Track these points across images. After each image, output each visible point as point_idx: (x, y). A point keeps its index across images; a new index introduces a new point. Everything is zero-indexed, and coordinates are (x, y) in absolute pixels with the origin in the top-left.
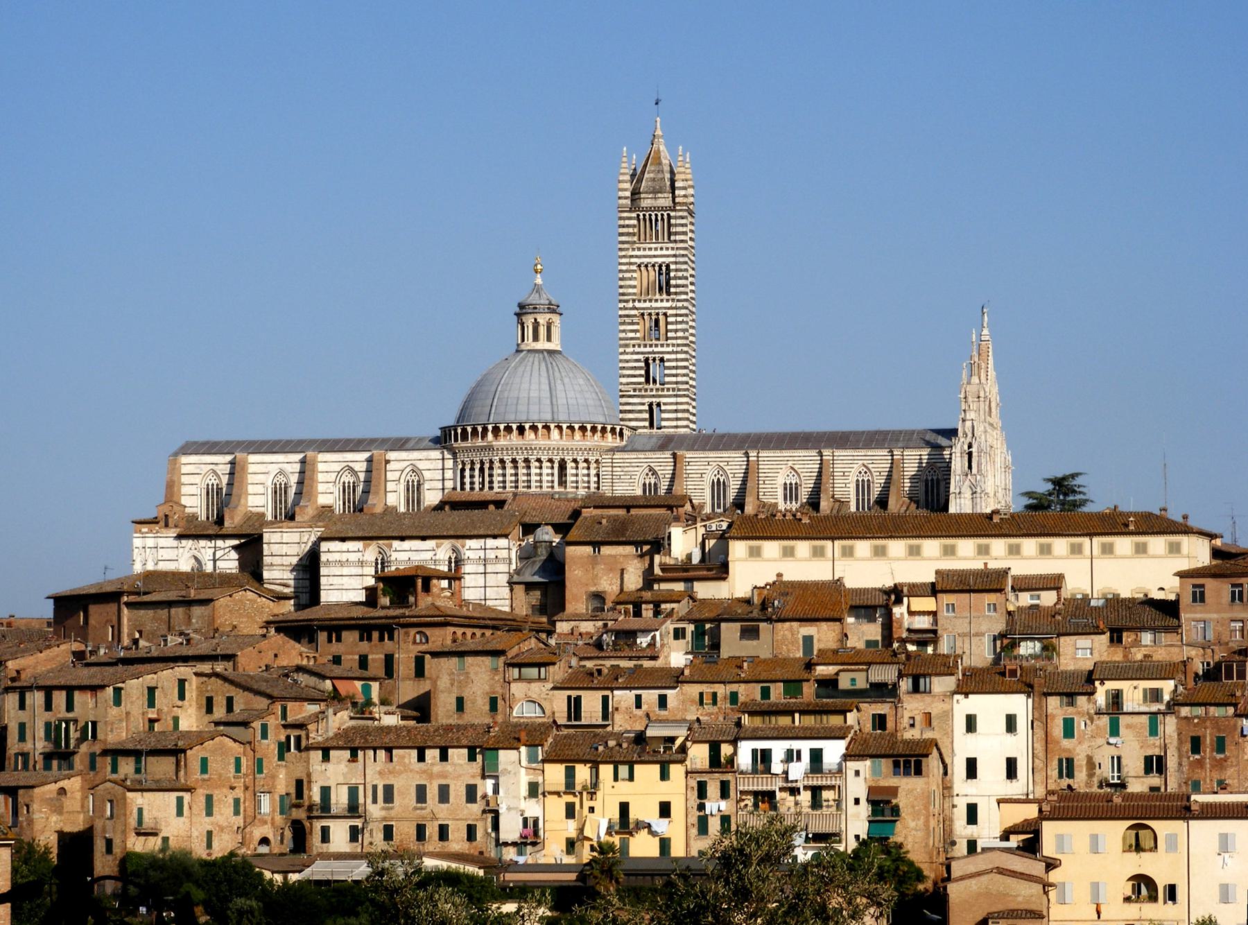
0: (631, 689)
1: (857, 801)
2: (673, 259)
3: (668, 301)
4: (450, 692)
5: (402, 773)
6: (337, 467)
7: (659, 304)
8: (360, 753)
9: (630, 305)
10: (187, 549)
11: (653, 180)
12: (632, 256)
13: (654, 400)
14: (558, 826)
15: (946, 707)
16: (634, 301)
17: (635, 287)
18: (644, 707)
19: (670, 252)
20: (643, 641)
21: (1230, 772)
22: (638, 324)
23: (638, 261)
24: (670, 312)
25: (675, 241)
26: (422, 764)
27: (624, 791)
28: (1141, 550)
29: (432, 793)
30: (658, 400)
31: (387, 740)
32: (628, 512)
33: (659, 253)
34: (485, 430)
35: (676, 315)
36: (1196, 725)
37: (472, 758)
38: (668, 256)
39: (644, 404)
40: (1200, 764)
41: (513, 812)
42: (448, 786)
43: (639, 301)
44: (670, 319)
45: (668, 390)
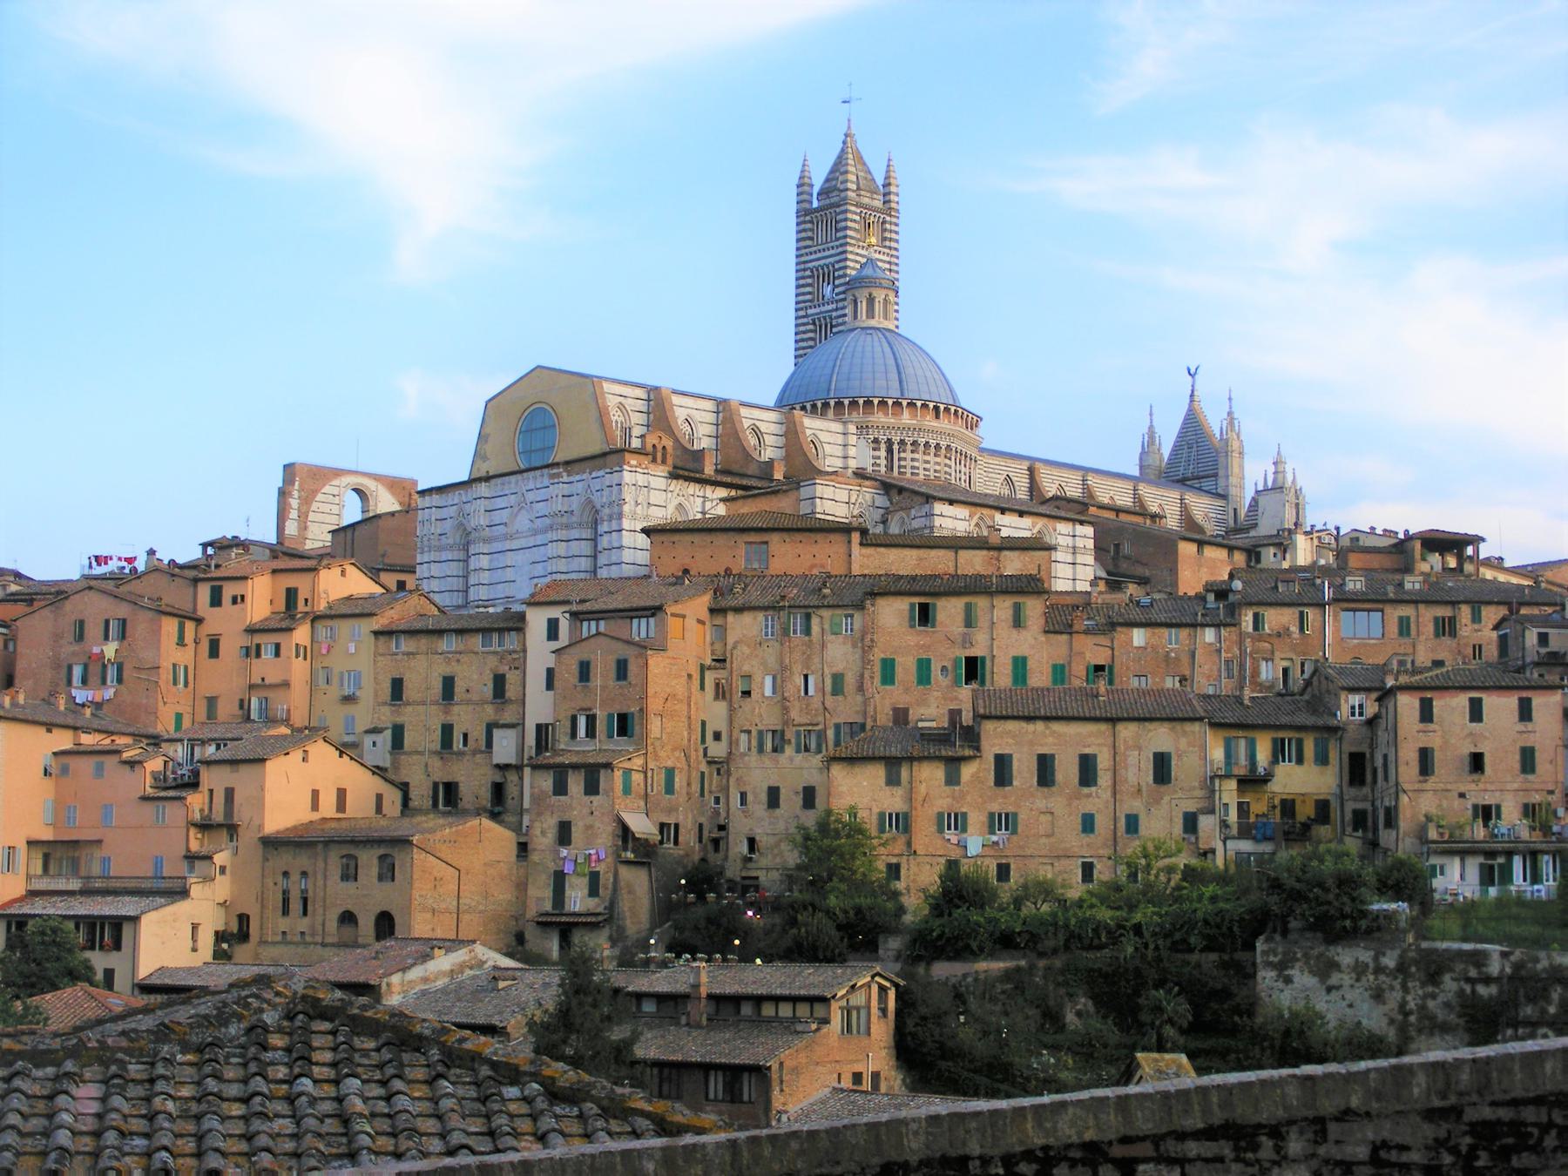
2: (887, 266)
10: (675, 494)
19: (888, 259)
25: (890, 248)
38: (884, 262)
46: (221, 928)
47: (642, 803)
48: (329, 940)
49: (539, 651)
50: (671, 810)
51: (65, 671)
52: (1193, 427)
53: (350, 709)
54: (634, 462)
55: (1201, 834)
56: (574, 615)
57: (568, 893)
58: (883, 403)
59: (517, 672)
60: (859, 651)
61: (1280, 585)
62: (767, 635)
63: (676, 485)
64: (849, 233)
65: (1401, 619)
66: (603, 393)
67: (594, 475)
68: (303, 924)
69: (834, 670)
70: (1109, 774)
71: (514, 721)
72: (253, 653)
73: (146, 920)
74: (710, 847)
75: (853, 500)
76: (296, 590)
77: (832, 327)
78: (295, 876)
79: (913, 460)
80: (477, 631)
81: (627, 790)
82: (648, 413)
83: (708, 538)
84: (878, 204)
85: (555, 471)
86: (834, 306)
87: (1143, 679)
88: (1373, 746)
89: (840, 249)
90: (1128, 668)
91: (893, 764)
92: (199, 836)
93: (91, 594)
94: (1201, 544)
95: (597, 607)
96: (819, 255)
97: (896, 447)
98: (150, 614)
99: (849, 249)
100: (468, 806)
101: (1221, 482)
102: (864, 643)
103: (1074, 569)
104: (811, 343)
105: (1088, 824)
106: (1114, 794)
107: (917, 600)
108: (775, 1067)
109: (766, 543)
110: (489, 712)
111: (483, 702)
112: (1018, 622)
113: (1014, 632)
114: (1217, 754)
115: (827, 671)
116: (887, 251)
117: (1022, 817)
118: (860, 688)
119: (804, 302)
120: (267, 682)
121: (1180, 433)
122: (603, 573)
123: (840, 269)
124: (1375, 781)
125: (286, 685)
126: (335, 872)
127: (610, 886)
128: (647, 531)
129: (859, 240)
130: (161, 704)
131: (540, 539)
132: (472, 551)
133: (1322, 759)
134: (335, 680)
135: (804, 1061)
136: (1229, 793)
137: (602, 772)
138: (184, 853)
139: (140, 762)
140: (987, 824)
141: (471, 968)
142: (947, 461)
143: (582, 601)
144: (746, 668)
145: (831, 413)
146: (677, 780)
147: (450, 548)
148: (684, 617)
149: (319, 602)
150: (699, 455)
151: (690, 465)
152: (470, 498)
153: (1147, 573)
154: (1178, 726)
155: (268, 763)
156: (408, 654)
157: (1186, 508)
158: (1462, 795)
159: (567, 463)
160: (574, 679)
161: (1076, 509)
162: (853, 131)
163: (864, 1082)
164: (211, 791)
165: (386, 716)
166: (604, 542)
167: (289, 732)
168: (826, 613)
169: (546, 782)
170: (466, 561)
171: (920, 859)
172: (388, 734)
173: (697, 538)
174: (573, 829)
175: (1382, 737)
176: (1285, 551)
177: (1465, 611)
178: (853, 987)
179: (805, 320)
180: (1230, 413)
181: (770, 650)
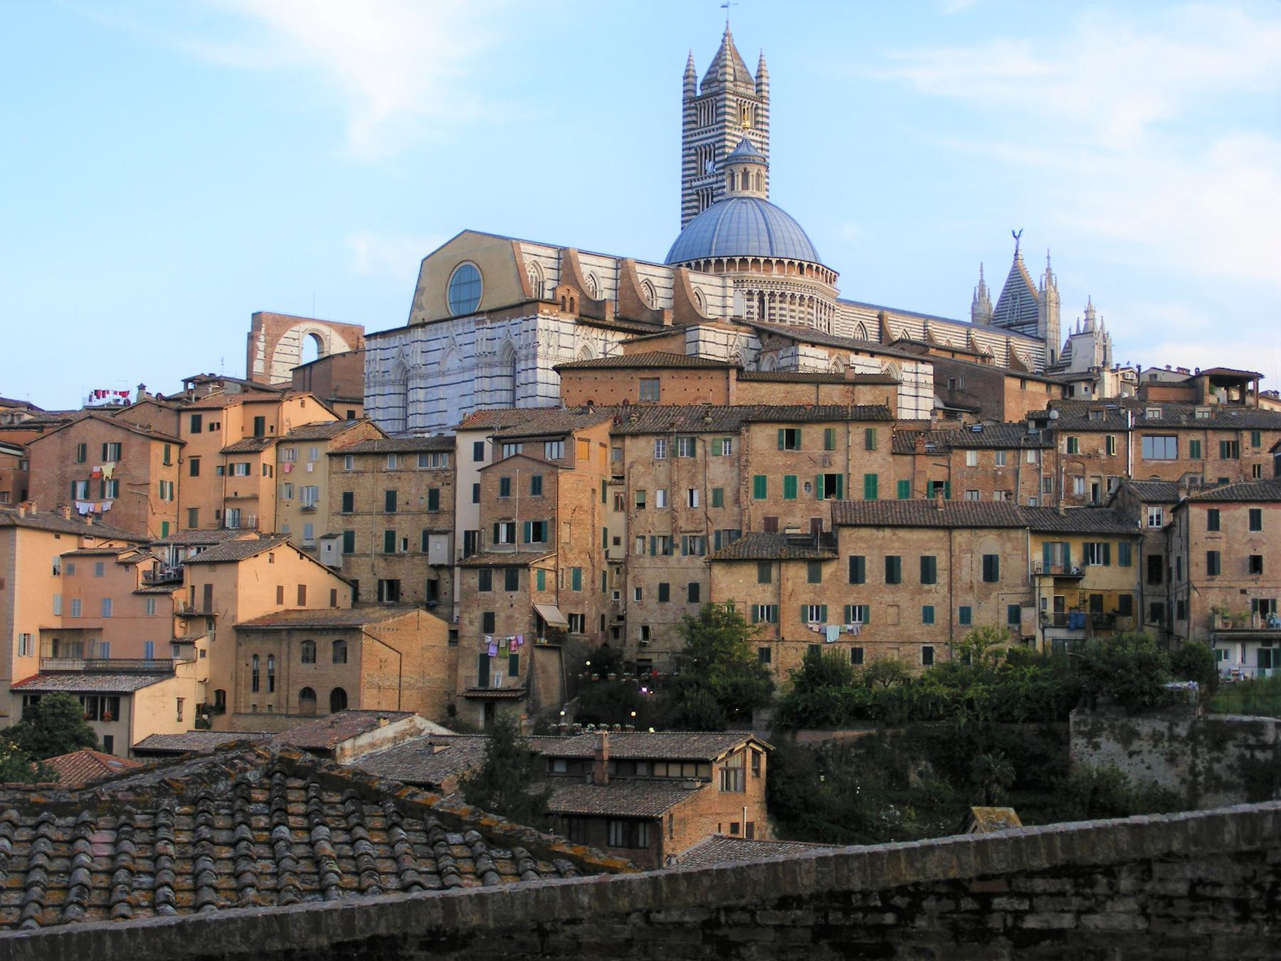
2: (760, 145)
10: (581, 337)
19: (760, 139)
25: (762, 130)
38: (757, 142)
46: (202, 702)
47: (554, 597)
48: (291, 712)
49: (467, 470)
50: (579, 603)
51: (70, 487)
52: (1017, 281)
53: (308, 518)
54: (546, 311)
55: (1023, 624)
56: (496, 439)
57: (491, 673)
58: (756, 261)
59: (449, 487)
60: (736, 470)
61: (1090, 414)
62: (658, 454)
63: (582, 330)
64: (728, 117)
65: (1192, 442)
66: (520, 253)
67: (513, 321)
68: (271, 699)
69: (716, 485)
70: (946, 573)
71: (447, 529)
72: (228, 471)
73: (138, 695)
74: (611, 634)
75: (731, 343)
76: (263, 418)
77: (713, 197)
78: (263, 659)
79: (781, 309)
80: (415, 453)
81: (541, 587)
82: (559, 270)
83: (609, 374)
84: (752, 92)
85: (480, 318)
86: (715, 179)
87: (975, 493)
88: (1168, 550)
89: (720, 131)
90: (962, 485)
91: (764, 565)
92: (183, 625)
93: (92, 421)
94: (1024, 380)
95: (515, 433)
96: (702, 136)
97: (766, 298)
98: (141, 439)
99: (727, 131)
100: (408, 600)
101: (1041, 327)
102: (740, 462)
103: (917, 401)
104: (695, 210)
105: (928, 615)
106: (951, 590)
107: (784, 427)
108: (666, 818)
109: (658, 379)
110: (426, 521)
111: (420, 513)
112: (869, 445)
113: (867, 453)
114: (1037, 556)
115: (709, 486)
116: (759, 132)
117: (872, 609)
118: (737, 501)
119: (689, 176)
120: (239, 495)
121: (1006, 286)
122: (521, 404)
123: (720, 148)
124: (1170, 579)
125: (255, 498)
126: (297, 655)
127: (527, 667)
128: (557, 369)
129: (735, 123)
130: (150, 514)
131: (467, 376)
132: (410, 386)
133: (1125, 561)
134: (296, 495)
135: (690, 813)
136: (1047, 589)
137: (521, 571)
138: (170, 639)
139: (133, 563)
140: (843, 615)
141: (411, 736)
142: (810, 310)
143: (503, 428)
144: (641, 484)
145: (712, 269)
146: (583, 578)
147: (393, 383)
148: (589, 441)
149: (282, 429)
150: (601, 305)
151: (594, 314)
152: (409, 342)
153: (978, 404)
154: (1004, 533)
155: (240, 563)
156: (357, 472)
157: (1011, 349)
158: (1243, 592)
159: (490, 312)
160: (497, 494)
161: (918, 350)
162: (731, 31)
163: (741, 831)
164: (193, 587)
165: (339, 525)
166: (521, 378)
167: (257, 537)
168: (708, 438)
169: (474, 580)
170: (406, 394)
171: (787, 644)
172: (341, 538)
173: (599, 375)
174: (496, 619)
175: (1176, 542)
176: (1094, 386)
177: (1247, 436)
178: (731, 751)
179: (690, 191)
180: (1048, 270)
181: (661, 468)
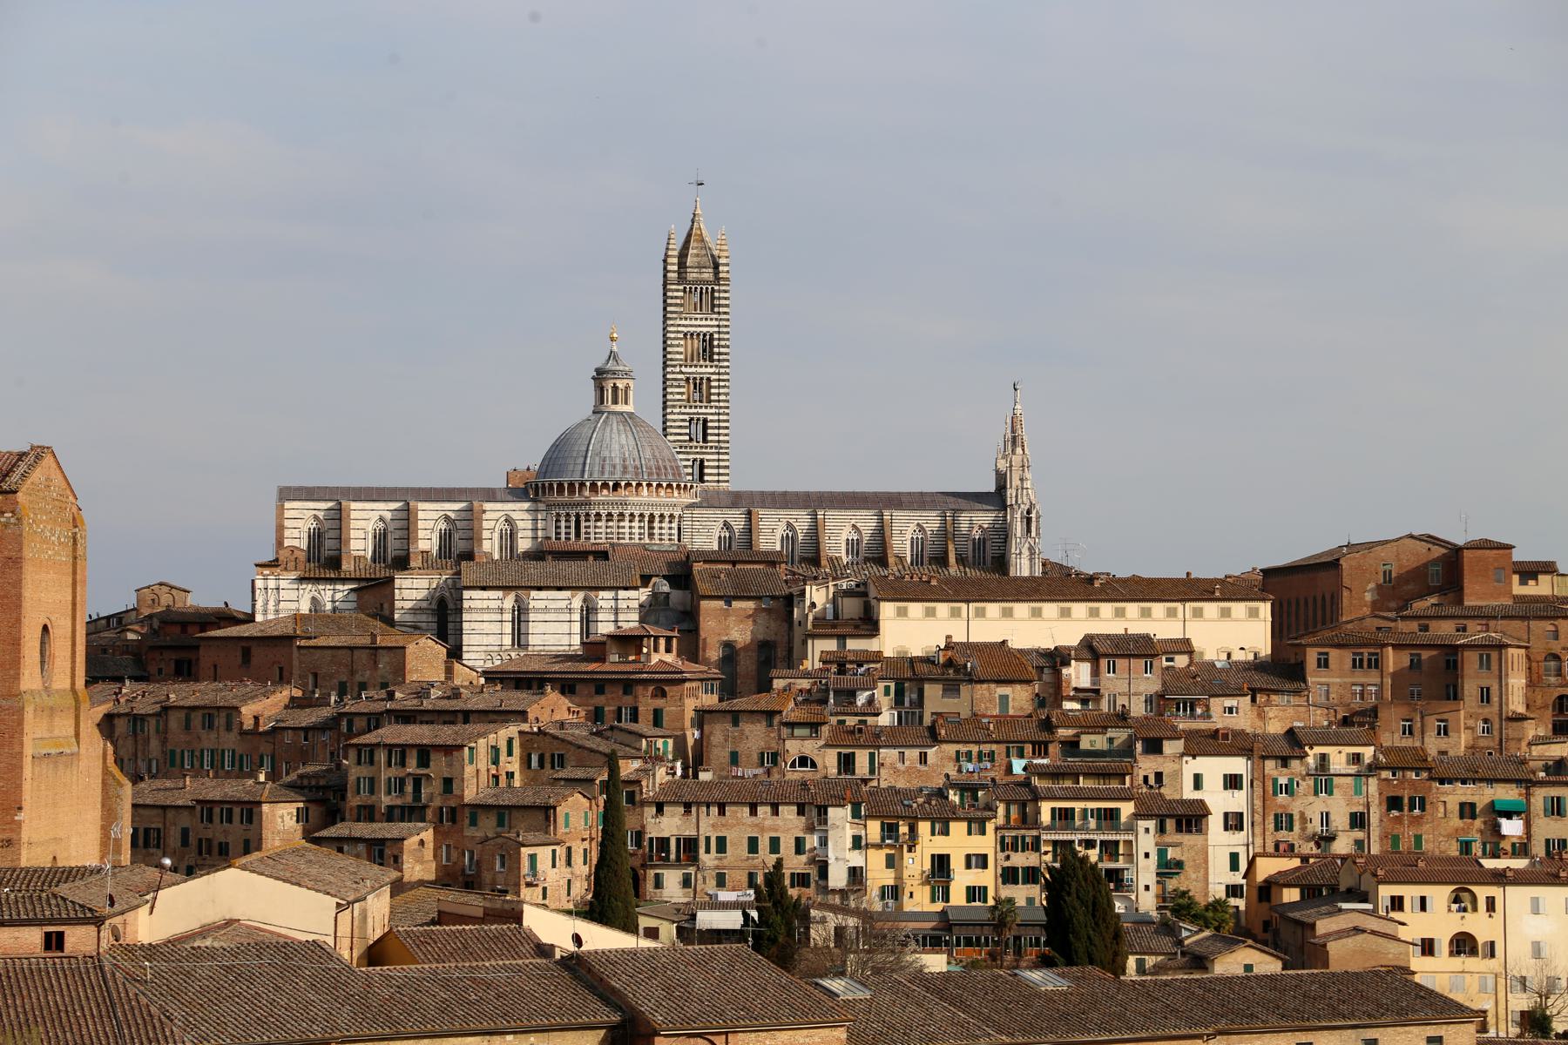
0: (894, 747)
1: (1147, 855)
2: (716, 329)
3: (711, 367)
4: (723, 747)
5: (735, 825)
6: (436, 515)
7: (703, 370)
8: (694, 809)
9: (678, 369)
10: (307, 590)
11: (697, 255)
12: (679, 325)
13: (698, 456)
14: (878, 875)
15: (1176, 766)
16: (681, 366)
17: (681, 353)
18: (907, 763)
19: (717, 323)
20: (862, 699)
21: (1426, 827)
22: (684, 387)
23: (685, 329)
24: (713, 377)
25: (719, 313)
26: (754, 818)
27: (940, 845)
28: (1226, 614)
29: (764, 844)
30: (702, 457)
31: (717, 795)
32: (734, 566)
33: (704, 324)
34: (582, 485)
35: (719, 380)
36: (1395, 786)
37: (801, 812)
38: (712, 326)
39: (689, 460)
40: (1398, 820)
41: (841, 862)
42: (779, 838)
43: (686, 366)
44: (713, 384)
45: (711, 447)
54: (268, 572)
84: (708, 275)
168: (149, 719)
